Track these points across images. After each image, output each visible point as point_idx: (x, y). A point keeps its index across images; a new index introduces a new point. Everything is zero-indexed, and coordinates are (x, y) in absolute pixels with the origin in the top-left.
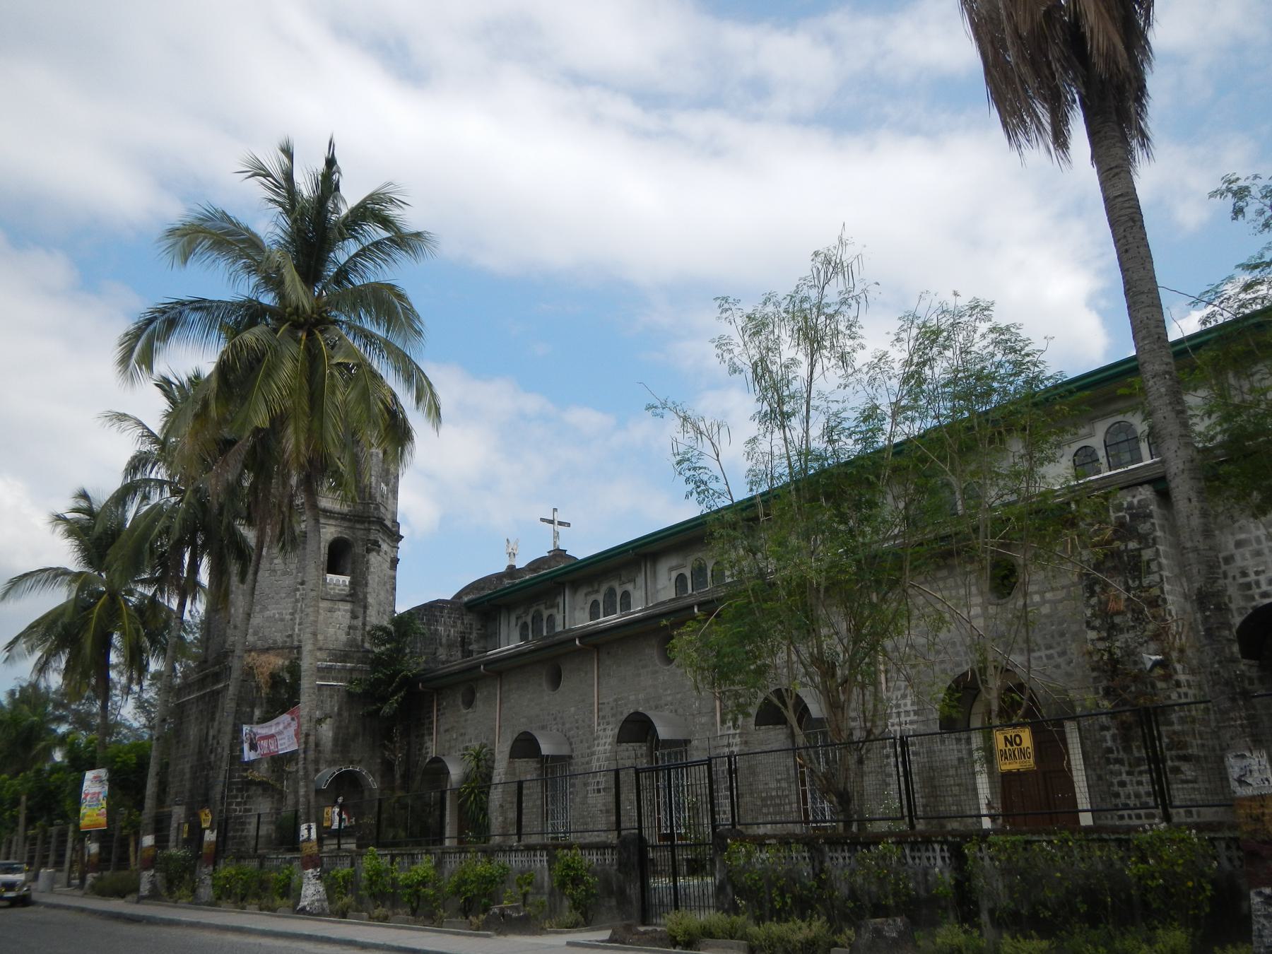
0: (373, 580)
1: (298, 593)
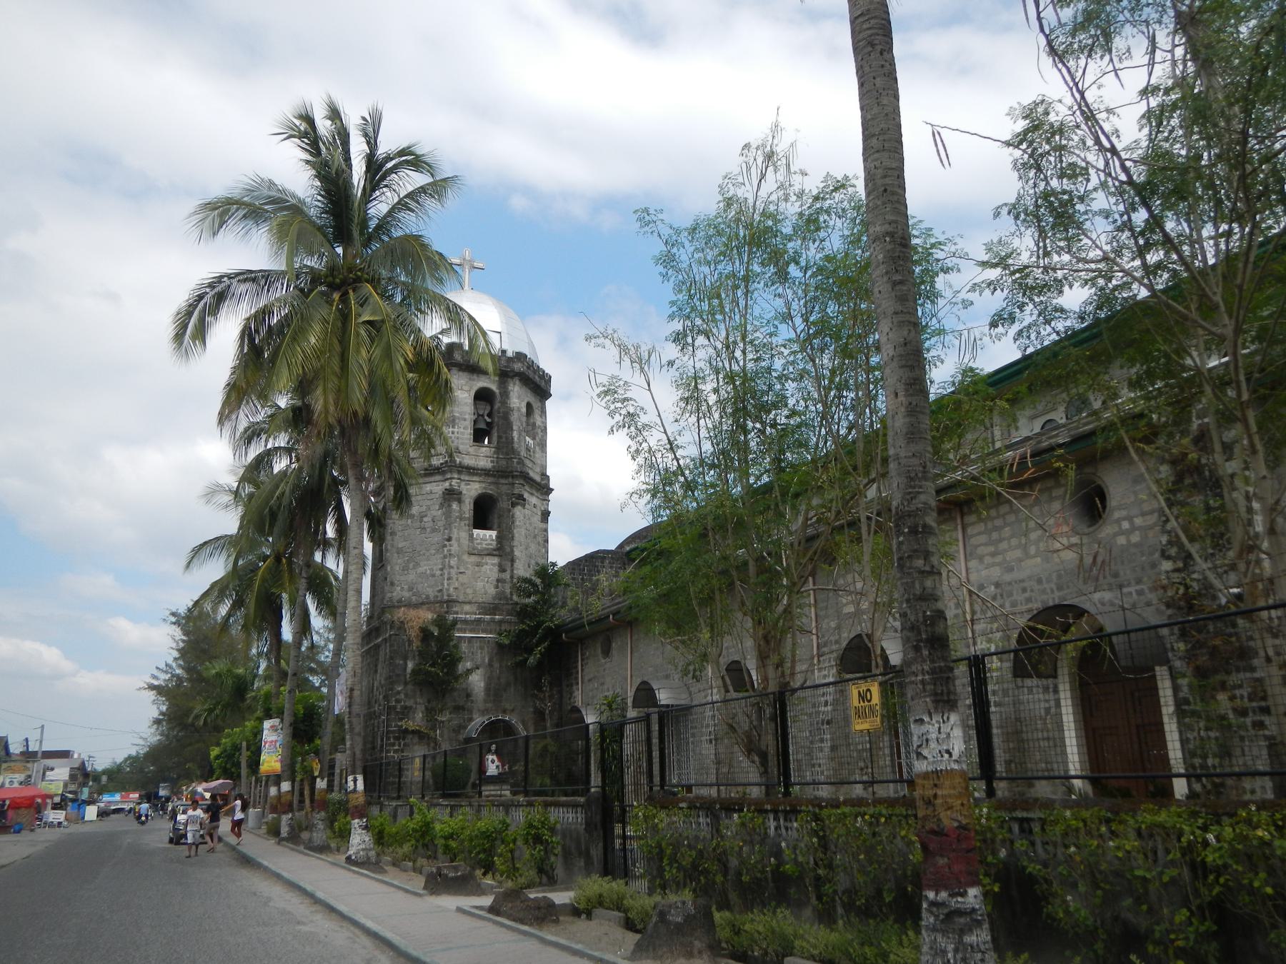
0: (520, 534)
1: (445, 549)
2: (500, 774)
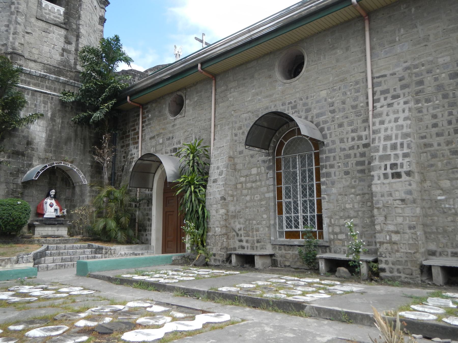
1: (13, 7)
2: (58, 217)
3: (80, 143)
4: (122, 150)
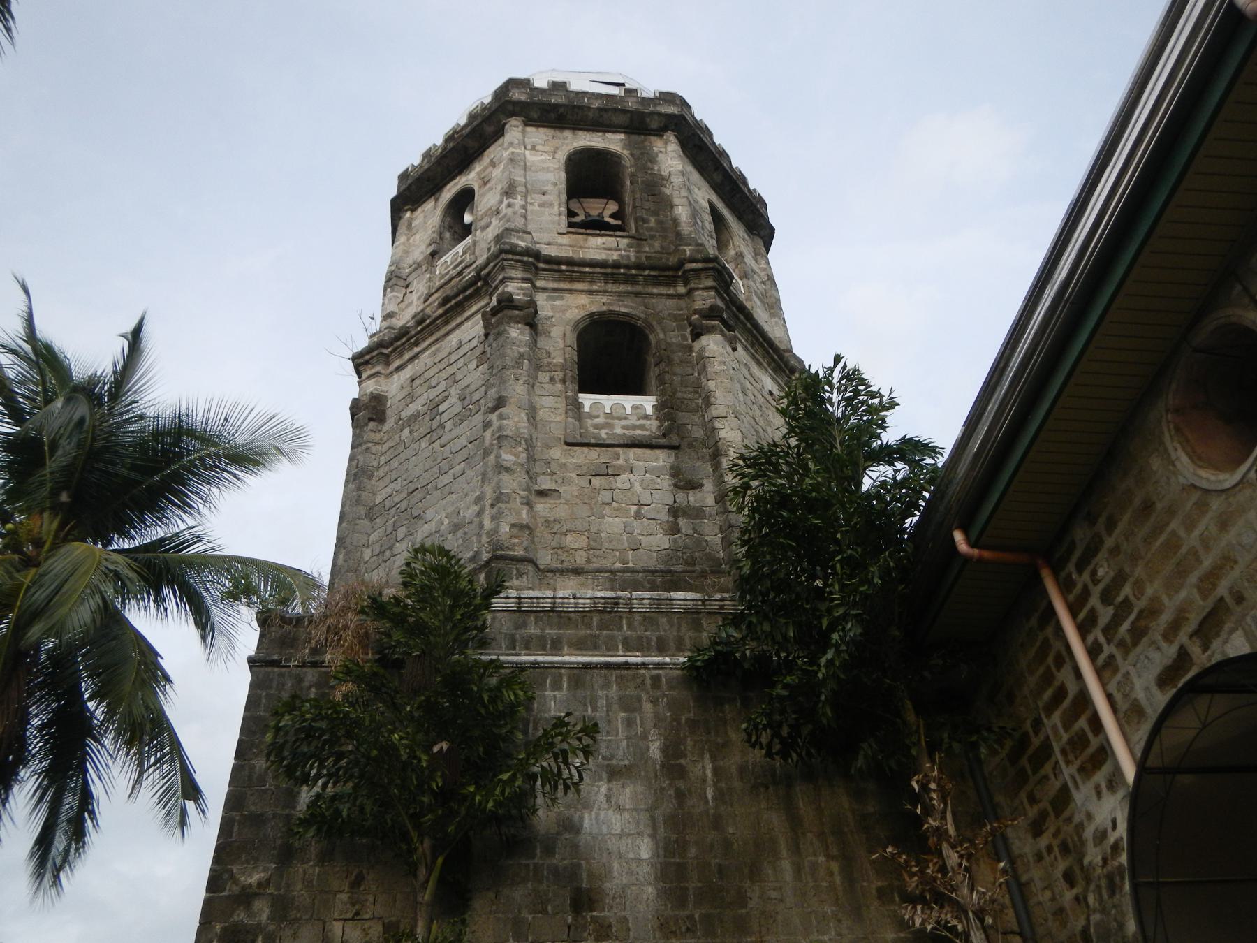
3: (821, 859)
4: (1043, 842)
